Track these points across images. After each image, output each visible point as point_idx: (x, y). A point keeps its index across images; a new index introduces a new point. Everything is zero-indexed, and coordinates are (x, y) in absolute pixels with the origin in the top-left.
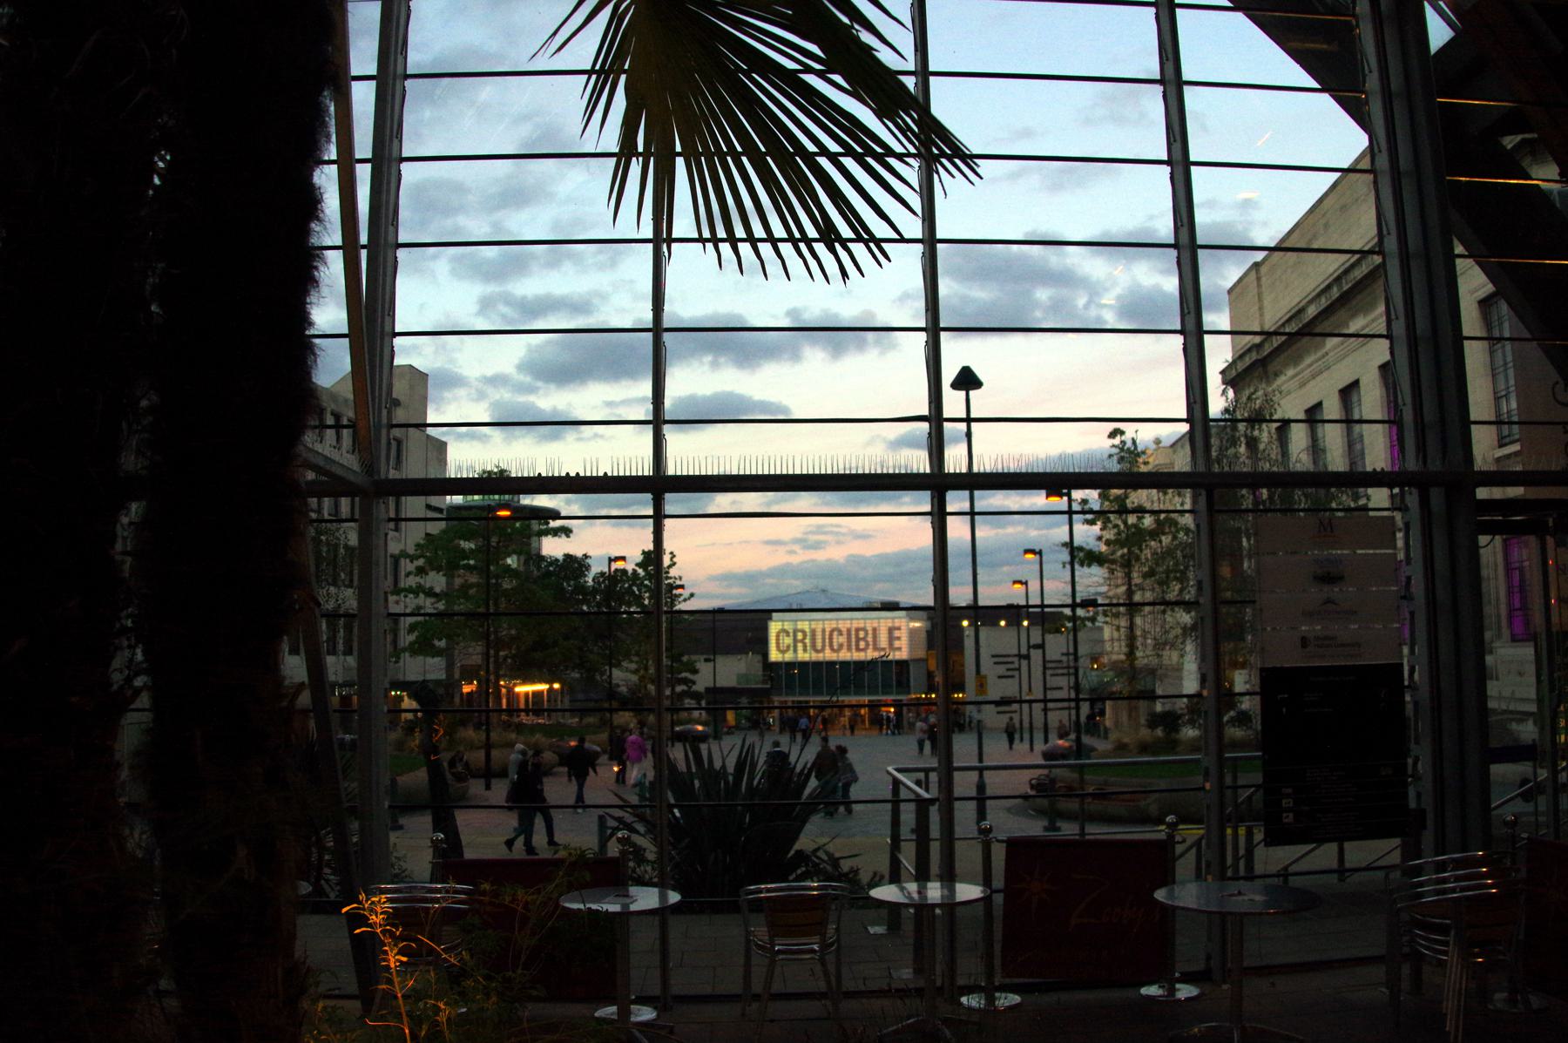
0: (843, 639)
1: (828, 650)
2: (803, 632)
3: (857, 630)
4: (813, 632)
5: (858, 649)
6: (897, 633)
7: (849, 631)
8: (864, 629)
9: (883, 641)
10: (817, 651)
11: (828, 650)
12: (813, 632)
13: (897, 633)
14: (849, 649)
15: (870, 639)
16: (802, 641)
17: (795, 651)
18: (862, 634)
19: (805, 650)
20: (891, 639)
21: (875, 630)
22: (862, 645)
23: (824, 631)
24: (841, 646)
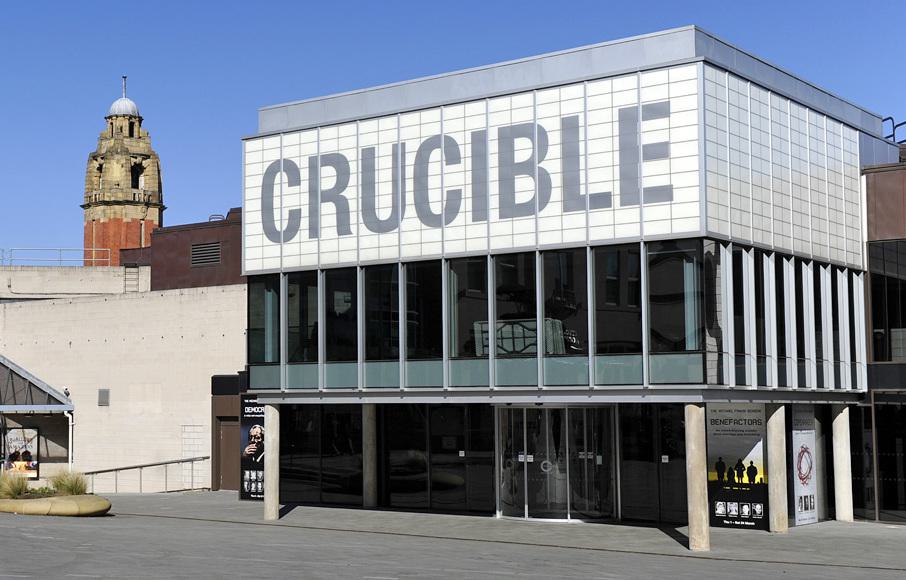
0: (459, 177)
1: (411, 219)
2: (337, 161)
3: (508, 135)
4: (368, 156)
5: (510, 209)
6: (650, 132)
7: (479, 139)
8: (524, 130)
9: (601, 172)
10: (379, 227)
11: (411, 219)
12: (368, 156)
13: (650, 132)
14: (480, 213)
15: (553, 164)
16: (335, 196)
17: (314, 232)
18: (523, 150)
19: (343, 228)
20: (631, 153)
21: (570, 126)
22: (525, 188)
23: (398, 152)
24: (453, 199)
